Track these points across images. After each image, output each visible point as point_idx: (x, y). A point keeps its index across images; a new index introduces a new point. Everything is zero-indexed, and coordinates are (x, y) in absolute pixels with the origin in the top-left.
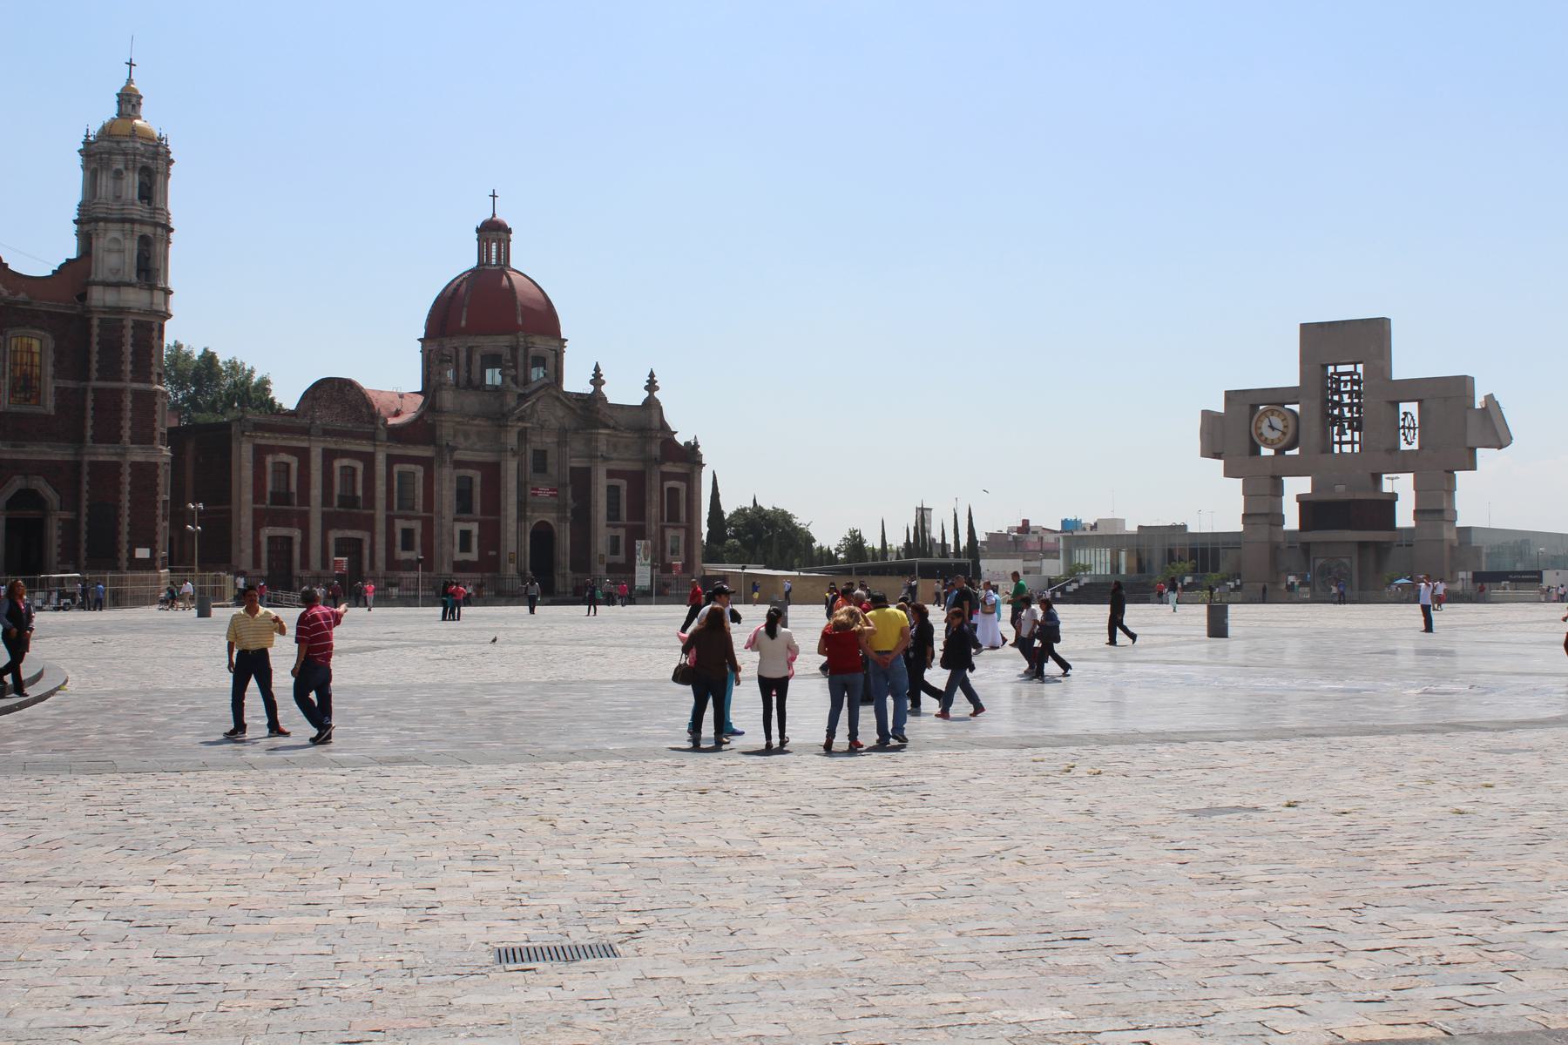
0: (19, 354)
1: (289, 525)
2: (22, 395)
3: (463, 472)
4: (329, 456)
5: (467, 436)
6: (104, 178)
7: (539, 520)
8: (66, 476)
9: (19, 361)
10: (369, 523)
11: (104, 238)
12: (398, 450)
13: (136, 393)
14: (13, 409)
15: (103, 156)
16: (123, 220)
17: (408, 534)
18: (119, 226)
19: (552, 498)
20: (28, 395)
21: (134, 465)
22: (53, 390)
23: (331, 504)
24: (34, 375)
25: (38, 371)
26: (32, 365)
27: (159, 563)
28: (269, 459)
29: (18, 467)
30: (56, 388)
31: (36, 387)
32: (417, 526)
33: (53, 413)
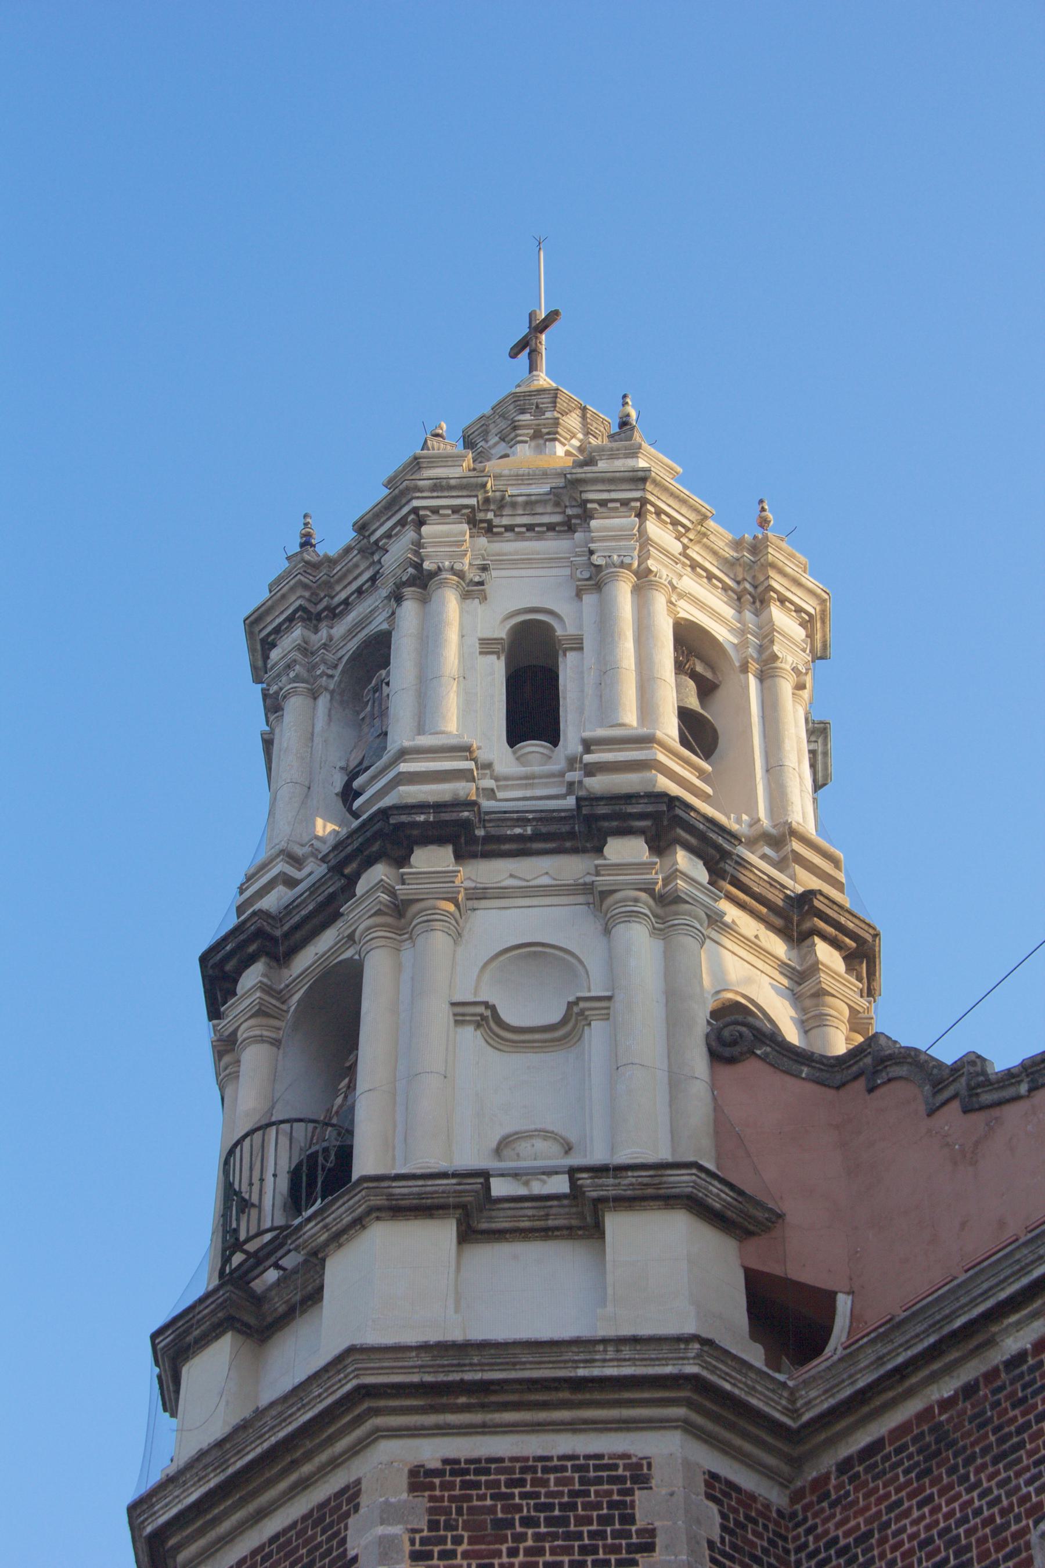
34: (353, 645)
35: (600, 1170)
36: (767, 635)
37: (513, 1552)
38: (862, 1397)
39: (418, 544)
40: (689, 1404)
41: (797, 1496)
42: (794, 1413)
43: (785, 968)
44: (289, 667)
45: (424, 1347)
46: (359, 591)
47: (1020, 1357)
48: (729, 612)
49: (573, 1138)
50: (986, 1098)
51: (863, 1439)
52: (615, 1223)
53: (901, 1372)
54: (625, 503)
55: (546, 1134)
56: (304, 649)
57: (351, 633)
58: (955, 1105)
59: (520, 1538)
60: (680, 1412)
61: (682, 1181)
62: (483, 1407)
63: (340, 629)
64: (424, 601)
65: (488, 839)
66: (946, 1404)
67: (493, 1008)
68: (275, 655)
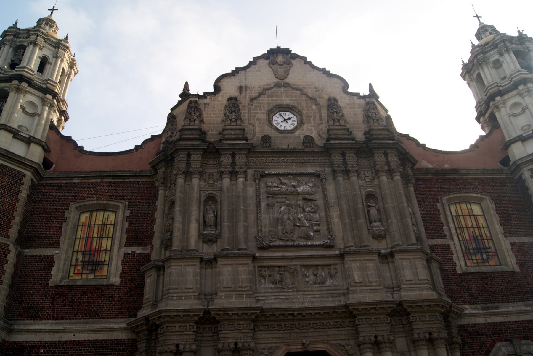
0: (461, 217)
2: (479, 257)
6: (486, 70)
9: (464, 226)
11: (505, 107)
15: (478, 57)
16: (515, 86)
18: (514, 92)
20: (485, 256)
22: (509, 247)
24: (484, 236)
25: (487, 232)
26: (479, 227)
30: (512, 244)
31: (490, 248)
33: (517, 269)
34: (19, 44)
35: (34, 138)
36: (71, 73)
37: (6, 178)
38: (53, 178)
39: (36, 39)
40: (34, 170)
41: (38, 184)
42: (44, 175)
43: (58, 119)
44: (9, 41)
45: (5, 150)
46: (23, 37)
47: (75, 183)
48: (67, 68)
49: (29, 129)
50: (82, 152)
51: (50, 182)
52: (32, 145)
53: (59, 177)
54: (64, 49)
55: (26, 128)
56: (12, 40)
57: (20, 42)
58: (78, 150)
59: (8, 177)
60: (32, 171)
61: (43, 144)
62: (9, 160)
63: (18, 40)
64: (34, 46)
65: (33, 85)
66: (63, 183)
67: (25, 108)
68: (7, 37)
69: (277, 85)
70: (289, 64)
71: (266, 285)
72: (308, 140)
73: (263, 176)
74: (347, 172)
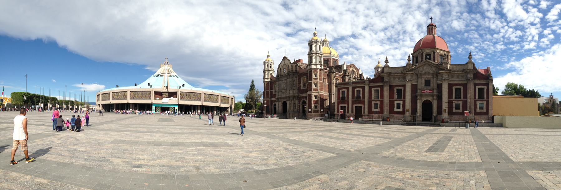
1: (345, 104)
3: (398, 88)
4: (353, 88)
5: (399, 78)
7: (425, 99)
8: (306, 97)
10: (364, 104)
12: (372, 85)
13: (309, 83)
14: (303, 89)
17: (376, 105)
19: (430, 93)
21: (308, 95)
23: (354, 99)
27: (312, 112)
28: (341, 91)
29: (303, 97)
32: (378, 103)
69: (284, 64)
70: (285, 60)
71: (282, 94)
72: (285, 74)
73: (282, 81)
74: (288, 79)
